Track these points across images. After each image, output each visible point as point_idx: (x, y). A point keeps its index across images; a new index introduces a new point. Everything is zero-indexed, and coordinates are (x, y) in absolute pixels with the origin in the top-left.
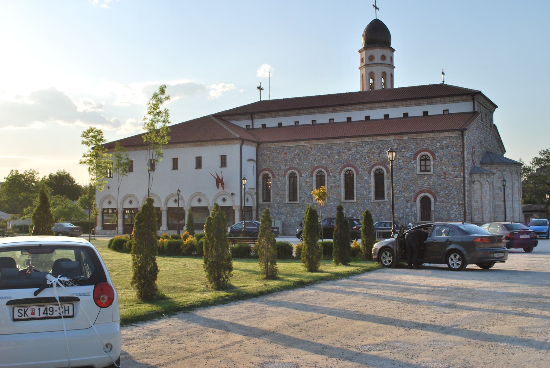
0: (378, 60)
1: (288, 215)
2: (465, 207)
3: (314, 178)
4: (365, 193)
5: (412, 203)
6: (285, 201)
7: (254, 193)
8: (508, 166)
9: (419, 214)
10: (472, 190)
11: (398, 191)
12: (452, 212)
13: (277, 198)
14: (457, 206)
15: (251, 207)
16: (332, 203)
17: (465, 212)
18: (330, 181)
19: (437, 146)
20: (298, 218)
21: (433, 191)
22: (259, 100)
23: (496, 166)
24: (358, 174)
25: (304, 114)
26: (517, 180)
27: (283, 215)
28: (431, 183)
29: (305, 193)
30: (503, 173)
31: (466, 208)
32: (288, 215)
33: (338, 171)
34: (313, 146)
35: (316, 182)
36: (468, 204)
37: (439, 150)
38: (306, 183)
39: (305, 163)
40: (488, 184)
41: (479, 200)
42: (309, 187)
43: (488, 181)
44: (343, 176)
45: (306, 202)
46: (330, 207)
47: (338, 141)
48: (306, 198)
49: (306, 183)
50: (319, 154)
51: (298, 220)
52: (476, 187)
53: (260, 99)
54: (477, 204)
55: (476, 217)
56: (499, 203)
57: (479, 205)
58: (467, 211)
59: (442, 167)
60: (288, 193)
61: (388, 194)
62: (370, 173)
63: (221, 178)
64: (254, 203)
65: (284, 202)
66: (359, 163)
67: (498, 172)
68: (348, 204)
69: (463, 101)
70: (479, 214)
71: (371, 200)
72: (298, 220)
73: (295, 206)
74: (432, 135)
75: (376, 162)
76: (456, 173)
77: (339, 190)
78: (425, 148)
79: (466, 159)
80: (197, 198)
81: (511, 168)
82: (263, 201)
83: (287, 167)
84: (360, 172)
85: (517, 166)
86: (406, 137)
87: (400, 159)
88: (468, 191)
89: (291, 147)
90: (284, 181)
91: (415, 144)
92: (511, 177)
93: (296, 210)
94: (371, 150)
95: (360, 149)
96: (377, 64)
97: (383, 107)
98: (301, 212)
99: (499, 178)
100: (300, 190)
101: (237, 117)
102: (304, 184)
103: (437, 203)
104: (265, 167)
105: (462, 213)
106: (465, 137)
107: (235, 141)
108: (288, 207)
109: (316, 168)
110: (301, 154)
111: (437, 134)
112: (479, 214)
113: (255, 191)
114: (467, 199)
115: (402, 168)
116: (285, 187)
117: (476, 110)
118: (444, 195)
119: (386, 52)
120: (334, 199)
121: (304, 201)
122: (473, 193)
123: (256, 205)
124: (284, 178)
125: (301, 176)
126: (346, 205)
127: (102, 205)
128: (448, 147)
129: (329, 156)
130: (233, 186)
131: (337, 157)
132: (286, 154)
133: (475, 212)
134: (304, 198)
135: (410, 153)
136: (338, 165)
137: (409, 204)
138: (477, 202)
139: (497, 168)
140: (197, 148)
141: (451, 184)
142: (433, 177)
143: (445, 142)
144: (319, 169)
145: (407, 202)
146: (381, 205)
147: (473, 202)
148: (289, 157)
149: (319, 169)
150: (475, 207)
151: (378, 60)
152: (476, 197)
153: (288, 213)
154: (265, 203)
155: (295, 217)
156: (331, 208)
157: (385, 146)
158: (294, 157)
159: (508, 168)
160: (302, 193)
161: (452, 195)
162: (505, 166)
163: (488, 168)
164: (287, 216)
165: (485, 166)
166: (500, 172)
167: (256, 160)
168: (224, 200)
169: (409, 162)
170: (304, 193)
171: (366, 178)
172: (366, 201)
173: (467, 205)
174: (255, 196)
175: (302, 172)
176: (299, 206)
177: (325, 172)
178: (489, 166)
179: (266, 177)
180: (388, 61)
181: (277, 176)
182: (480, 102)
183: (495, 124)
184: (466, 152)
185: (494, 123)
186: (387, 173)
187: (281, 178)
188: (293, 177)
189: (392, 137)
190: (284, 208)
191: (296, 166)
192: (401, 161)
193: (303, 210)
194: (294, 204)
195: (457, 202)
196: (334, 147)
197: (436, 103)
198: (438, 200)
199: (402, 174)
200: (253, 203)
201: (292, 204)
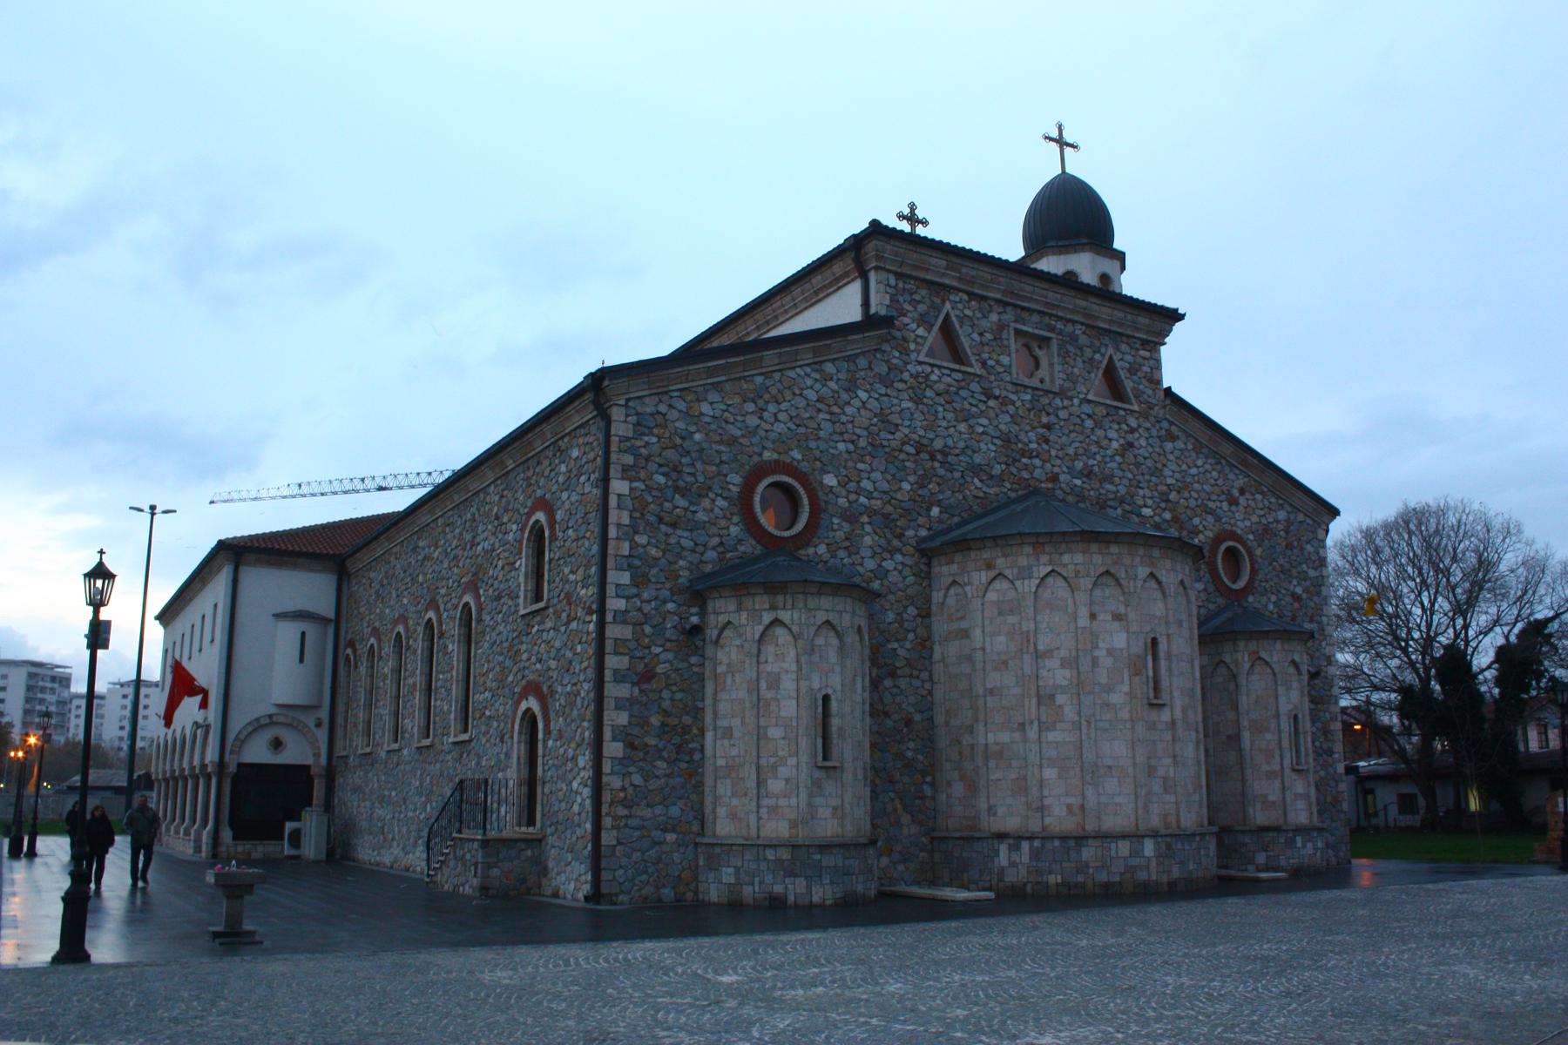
7: (311, 723)
8: (1047, 548)
10: (707, 674)
15: (305, 769)
23: (986, 555)
26: (1117, 617)
30: (1018, 583)
31: (607, 767)
36: (631, 746)
37: (565, 495)
40: (790, 638)
41: (736, 722)
43: (787, 621)
52: (725, 661)
54: (726, 742)
55: (722, 811)
56: (1005, 737)
57: (734, 752)
58: (613, 782)
64: (317, 755)
67: (997, 585)
70: (733, 795)
81: (1066, 558)
85: (1114, 549)
92: (1070, 601)
99: (1000, 614)
106: (617, 414)
112: (733, 795)
113: (324, 714)
114: (616, 718)
122: (709, 687)
123: (323, 760)
133: (719, 782)
138: (728, 734)
143: (575, 453)
147: (709, 736)
150: (721, 762)
152: (723, 708)
159: (1044, 558)
162: (1028, 549)
165: (943, 559)
166: (1006, 585)
167: (331, 614)
168: (277, 744)
173: (613, 749)
174: (322, 735)
178: (958, 557)
182: (929, 277)
183: (1170, 388)
184: (619, 486)
185: (1165, 385)
196: (421, 544)
200: (314, 755)
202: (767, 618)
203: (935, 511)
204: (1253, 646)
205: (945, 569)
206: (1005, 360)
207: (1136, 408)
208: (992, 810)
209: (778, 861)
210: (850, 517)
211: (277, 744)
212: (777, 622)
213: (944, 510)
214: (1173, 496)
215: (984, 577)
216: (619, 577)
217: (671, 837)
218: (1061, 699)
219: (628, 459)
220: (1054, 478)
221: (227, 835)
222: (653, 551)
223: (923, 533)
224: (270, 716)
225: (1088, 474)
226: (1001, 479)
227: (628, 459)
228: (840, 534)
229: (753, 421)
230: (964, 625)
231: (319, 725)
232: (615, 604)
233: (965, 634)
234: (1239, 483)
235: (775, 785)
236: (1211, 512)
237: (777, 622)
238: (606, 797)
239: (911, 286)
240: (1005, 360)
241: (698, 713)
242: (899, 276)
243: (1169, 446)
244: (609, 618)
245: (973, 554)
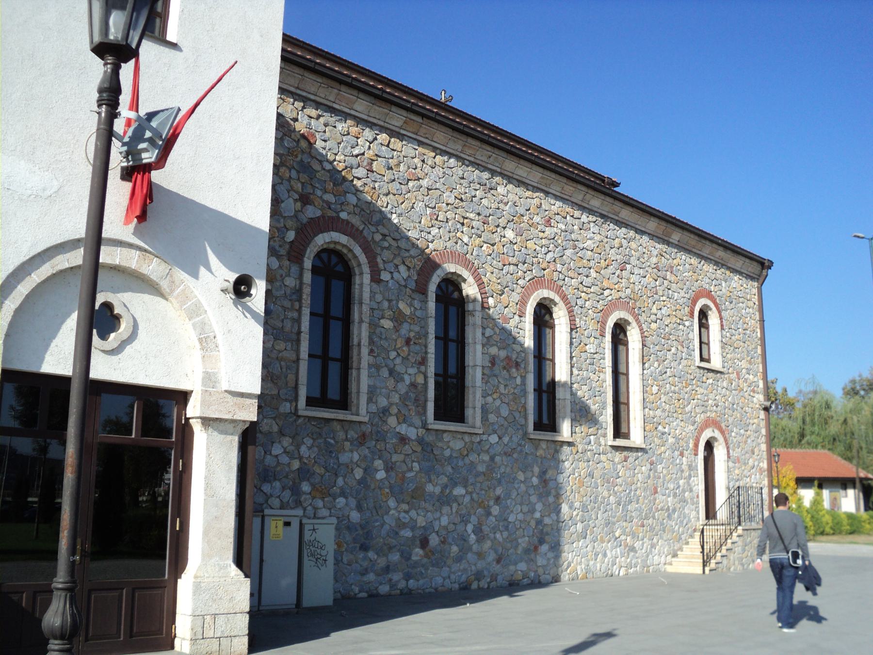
16: (494, 439)
20: (353, 502)
21: (723, 425)
27: (277, 484)
29: (391, 372)
32: (306, 487)
33: (516, 297)
38: (398, 318)
42: (408, 342)
45: (392, 421)
46: (486, 458)
48: (396, 399)
49: (398, 318)
51: (355, 516)
62: (603, 335)
65: (286, 408)
68: (544, 445)
71: (605, 436)
72: (355, 516)
73: (341, 435)
77: (519, 381)
83: (312, 212)
90: (290, 282)
93: (344, 458)
98: (369, 471)
102: (387, 324)
108: (309, 441)
116: (298, 321)
118: (739, 438)
120: (502, 421)
121: (385, 412)
124: (295, 269)
125: (376, 279)
126: (540, 452)
131: (510, 234)
134: (388, 398)
135: (682, 293)
146: (631, 460)
153: (304, 473)
155: (341, 501)
156: (492, 459)
160: (378, 367)
164: (296, 491)
170: (385, 373)
175: (379, 260)
176: (363, 439)
190: (286, 442)
191: (356, 221)
193: (378, 463)
194: (337, 426)
195: (756, 463)
199: (669, 356)
201: (328, 420)
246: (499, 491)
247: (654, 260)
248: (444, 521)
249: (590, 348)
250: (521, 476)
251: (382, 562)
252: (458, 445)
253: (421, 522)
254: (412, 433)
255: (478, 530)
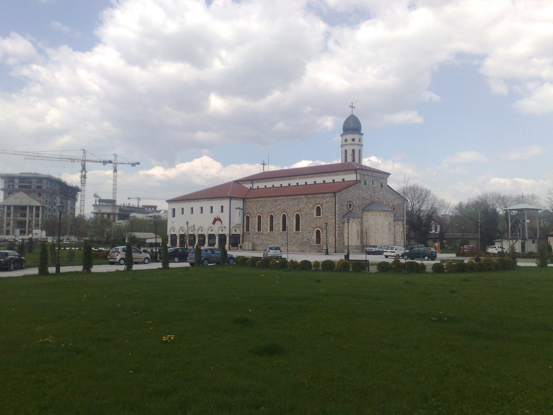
0: (349, 141)
1: (257, 239)
2: (335, 236)
3: (269, 219)
4: (291, 228)
5: (312, 234)
6: (255, 231)
9: (315, 240)
11: (306, 227)
12: (330, 239)
13: (252, 230)
14: (332, 236)
15: (239, 234)
16: (276, 233)
17: (336, 240)
18: (276, 220)
19: (324, 202)
21: (322, 227)
22: (263, 171)
24: (288, 217)
25: (277, 181)
26: (386, 220)
28: (321, 222)
31: (336, 237)
32: (257, 239)
33: (279, 215)
34: (268, 201)
35: (269, 221)
37: (325, 204)
38: (265, 221)
39: (265, 210)
44: (281, 218)
45: (265, 232)
47: (280, 198)
49: (265, 221)
50: (271, 205)
51: (261, 242)
53: (264, 170)
59: (326, 213)
60: (257, 227)
61: (301, 228)
63: (219, 218)
64: (241, 232)
66: (289, 210)
69: (351, 173)
71: (293, 231)
74: (321, 195)
75: (296, 210)
76: (332, 217)
78: (318, 202)
79: (337, 209)
80: (210, 230)
82: (247, 231)
83: (257, 212)
84: (289, 216)
86: (309, 196)
87: (307, 209)
88: (339, 227)
89: (259, 201)
91: (314, 200)
94: (294, 203)
95: (290, 202)
96: (349, 144)
97: (313, 177)
98: (263, 238)
100: (262, 225)
101: (245, 182)
102: (264, 222)
103: (323, 234)
104: (247, 212)
105: (334, 240)
106: (337, 196)
107: (227, 198)
109: (270, 213)
110: (263, 205)
111: (323, 195)
114: (337, 232)
115: (308, 214)
117: (358, 179)
119: (356, 137)
121: (264, 231)
122: (345, 229)
125: (263, 217)
127: (170, 232)
128: (329, 202)
129: (275, 207)
130: (226, 223)
131: (279, 207)
132: (256, 205)
135: (311, 205)
136: (279, 211)
137: (311, 234)
139: (371, 213)
140: (211, 202)
141: (330, 223)
142: (322, 219)
143: (327, 199)
144: (271, 214)
145: (310, 233)
147: (345, 234)
148: (258, 206)
149: (271, 214)
151: (349, 141)
154: (247, 232)
157: (300, 201)
158: (260, 207)
161: (330, 229)
163: (366, 213)
164: (256, 240)
169: (311, 210)
171: (291, 219)
172: (291, 232)
173: (337, 235)
176: (262, 235)
177: (274, 215)
179: (248, 217)
180: (357, 142)
181: (253, 217)
184: (337, 205)
185: (388, 184)
186: (301, 216)
187: (254, 218)
188: (259, 217)
189: (303, 196)
192: (307, 210)
193: (263, 237)
196: (278, 201)
197: (338, 175)
198: (324, 232)
199: (308, 217)
202: (353, 221)
203: (363, 205)
204: (397, 222)
205: (365, 213)
206: (371, 184)
207: (384, 188)
208: (371, 243)
209: (354, 248)
210: (356, 207)
211: (236, 230)
212: (354, 221)
213: (364, 205)
214: (388, 200)
215: (371, 215)
216: (337, 216)
217: (342, 245)
218: (380, 230)
219: (338, 202)
220: (375, 199)
221: (231, 246)
222: (340, 213)
223: (362, 208)
224: (235, 226)
225: (378, 199)
226: (369, 200)
227: (338, 202)
228: (355, 209)
229: (348, 196)
230: (368, 220)
231: (241, 227)
232: (337, 219)
233: (368, 221)
234: (395, 198)
235: (353, 240)
236: (392, 202)
237: (354, 221)
238: (336, 241)
239: (362, 175)
240: (371, 184)
241: (343, 231)
242: (361, 174)
243: (387, 193)
244: (336, 220)
245: (370, 212)
246: (277, 239)
247: (305, 202)
248: (270, 243)
249: (291, 219)
250: (280, 237)
251: (264, 247)
252: (272, 234)
253: (268, 243)
254: (267, 233)
255: (274, 243)
